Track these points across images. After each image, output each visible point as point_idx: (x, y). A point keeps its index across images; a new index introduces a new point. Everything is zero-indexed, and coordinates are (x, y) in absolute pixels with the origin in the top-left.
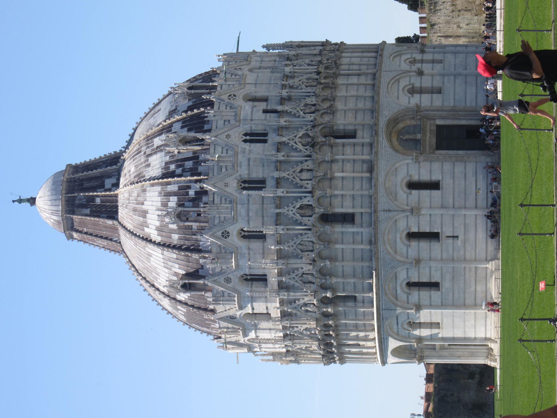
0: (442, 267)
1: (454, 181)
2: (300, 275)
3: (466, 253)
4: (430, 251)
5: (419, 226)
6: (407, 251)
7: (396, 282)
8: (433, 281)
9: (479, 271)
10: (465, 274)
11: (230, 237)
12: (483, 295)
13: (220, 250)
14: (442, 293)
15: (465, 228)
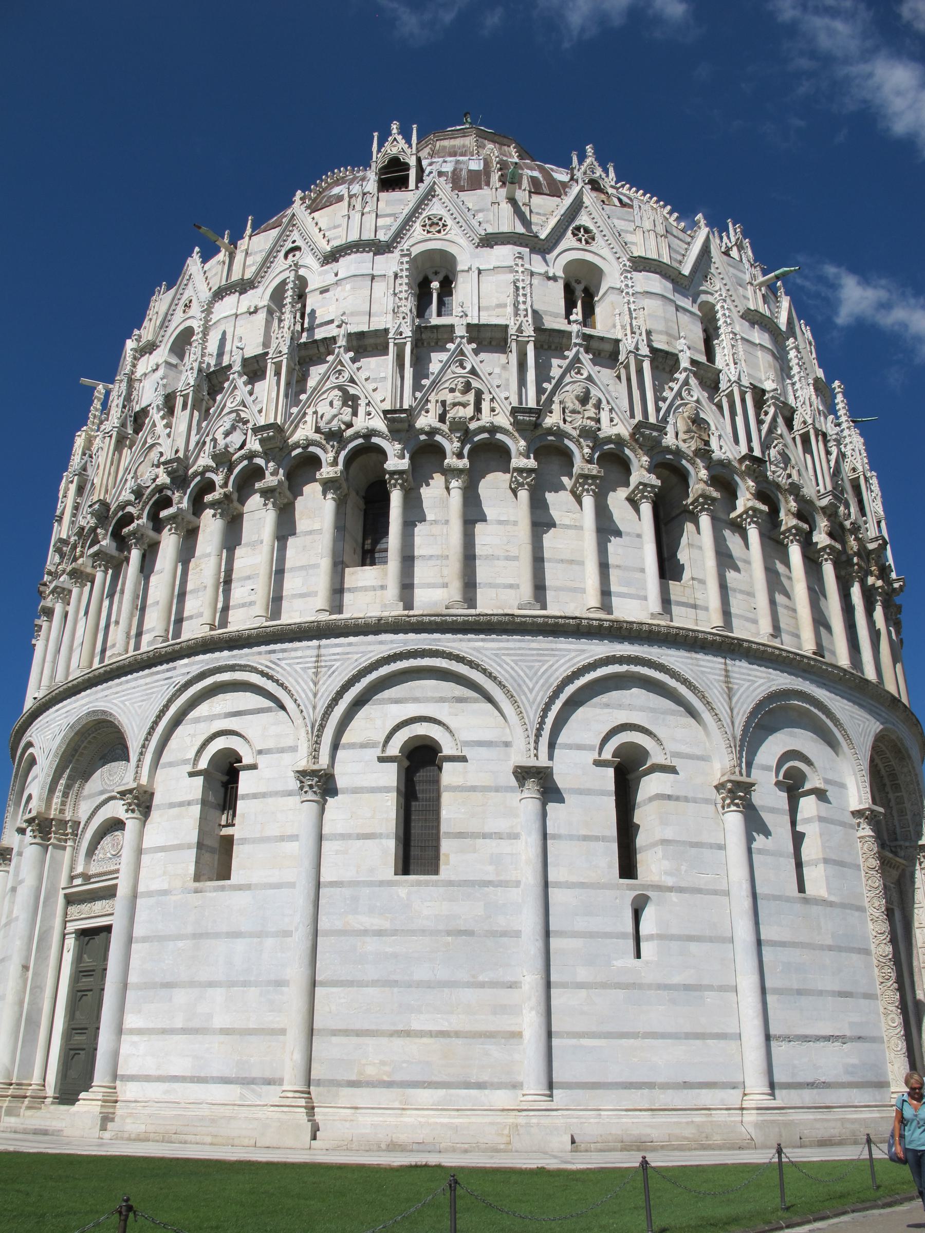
0: (517, 884)
1: (830, 948)
2: (475, 384)
3: (583, 993)
4: (586, 838)
5: (677, 799)
6: (579, 747)
7: (442, 700)
8: (446, 846)
9: (495, 1051)
10: (482, 985)
11: (577, 245)
12: (371, 1072)
13: (538, 214)
14: (381, 883)
15: (687, 988)
